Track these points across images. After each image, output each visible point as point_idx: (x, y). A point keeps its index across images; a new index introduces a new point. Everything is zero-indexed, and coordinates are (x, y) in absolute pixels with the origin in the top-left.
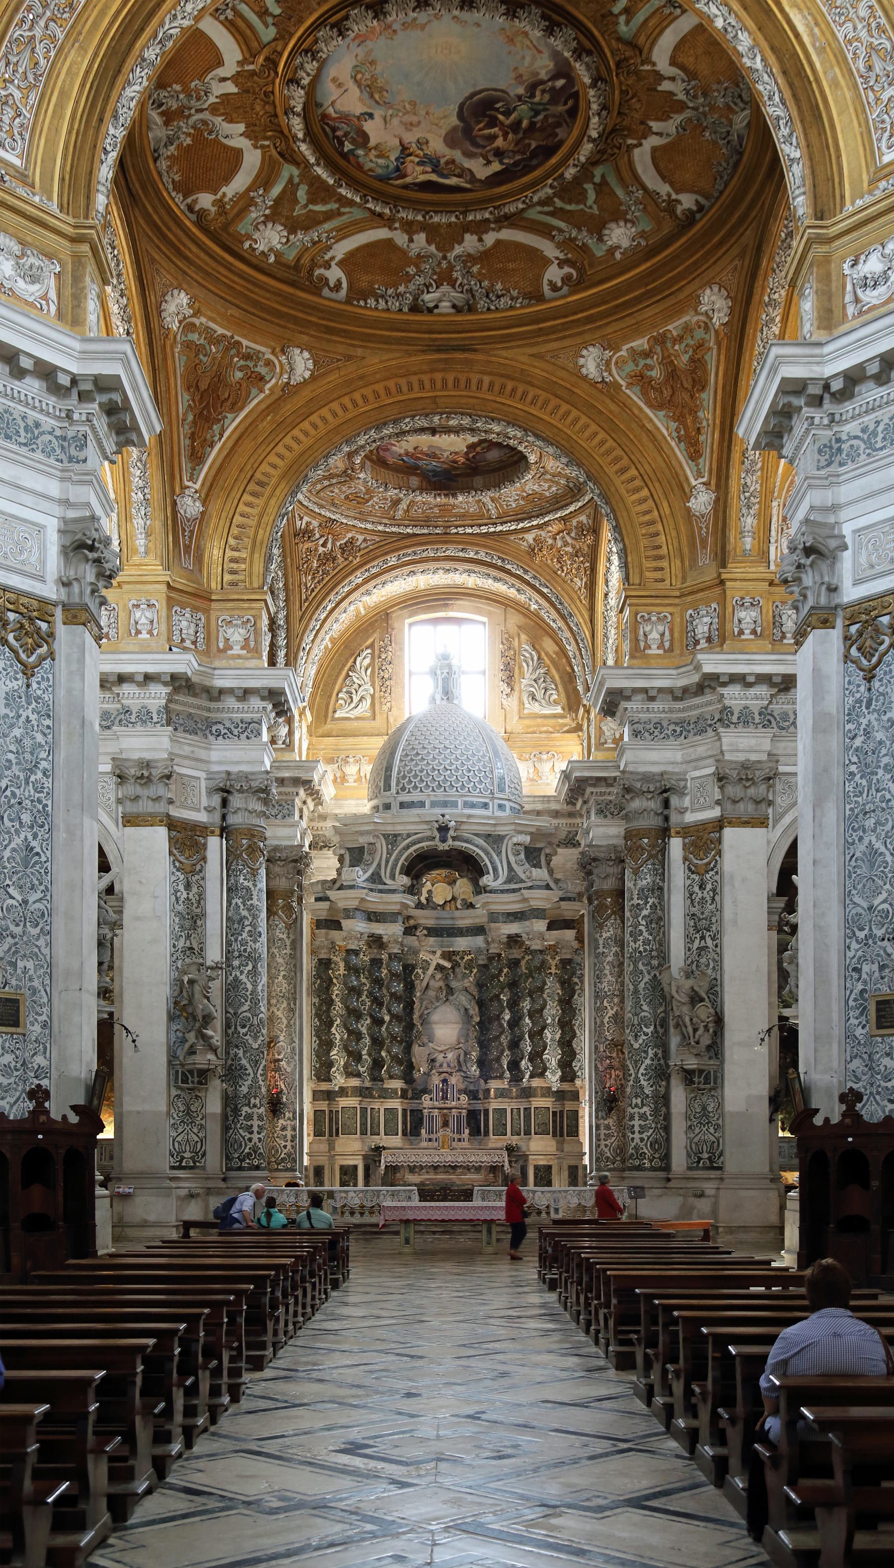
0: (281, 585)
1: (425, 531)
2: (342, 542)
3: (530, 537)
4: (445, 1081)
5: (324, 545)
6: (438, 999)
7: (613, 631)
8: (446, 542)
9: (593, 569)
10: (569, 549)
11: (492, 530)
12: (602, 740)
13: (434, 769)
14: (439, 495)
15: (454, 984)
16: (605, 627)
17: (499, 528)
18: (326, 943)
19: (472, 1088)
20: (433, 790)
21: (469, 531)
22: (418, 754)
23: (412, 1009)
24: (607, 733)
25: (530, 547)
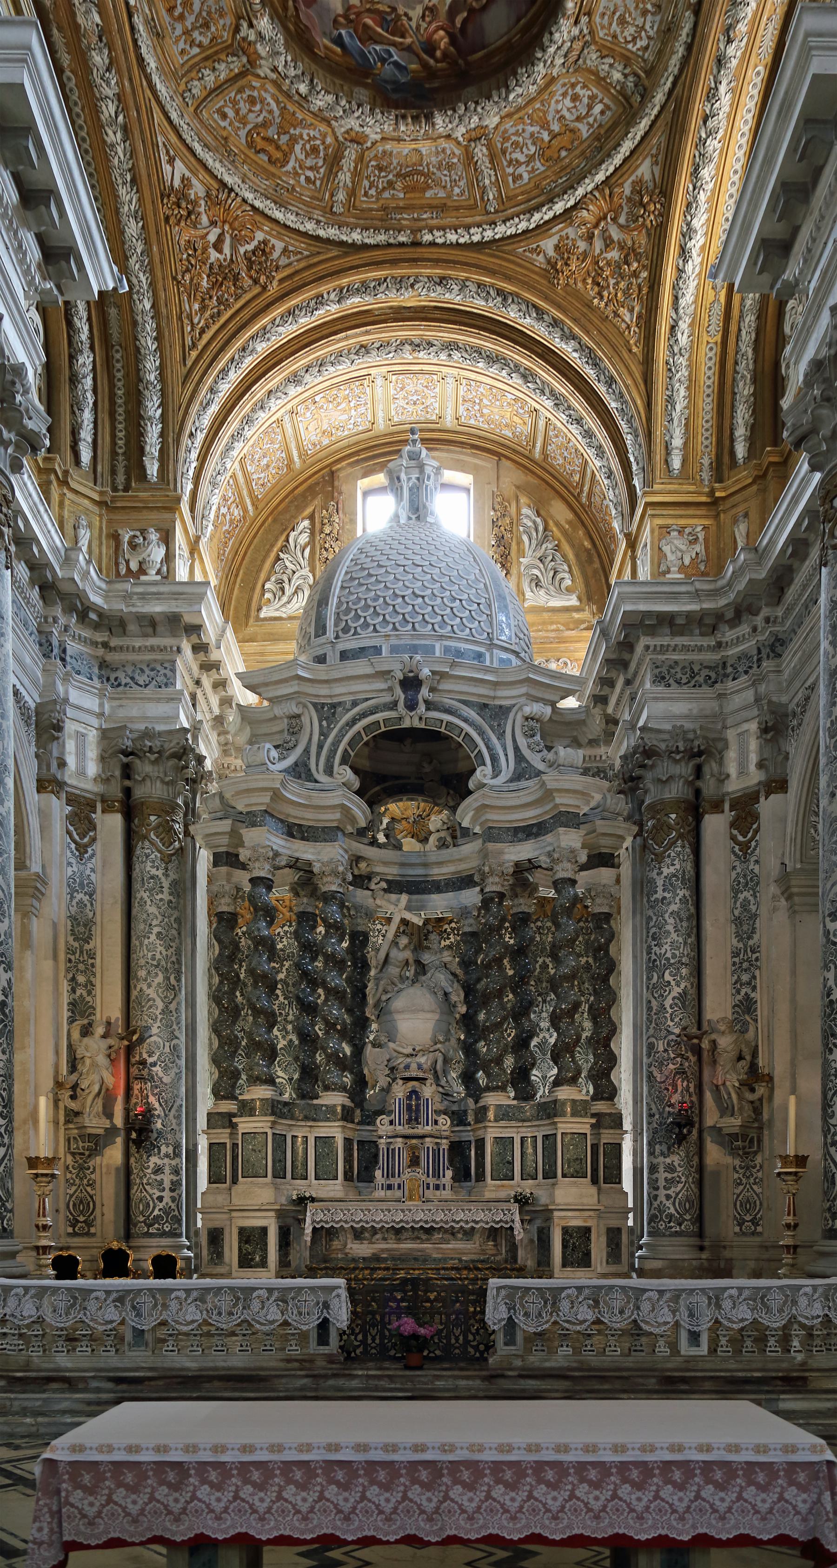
0: (148, 306)
1: (381, 238)
2: (250, 247)
3: (548, 245)
4: (414, 1094)
5: (218, 246)
6: (402, 979)
7: (682, 392)
8: (414, 261)
9: (655, 283)
10: (614, 255)
11: (489, 234)
12: (663, 568)
13: (395, 595)
14: (404, 117)
15: (426, 958)
16: (670, 387)
17: (502, 230)
18: (227, 888)
19: (455, 1108)
20: (395, 629)
21: (452, 237)
22: (370, 575)
23: (364, 996)
24: (671, 557)
25: (549, 262)
